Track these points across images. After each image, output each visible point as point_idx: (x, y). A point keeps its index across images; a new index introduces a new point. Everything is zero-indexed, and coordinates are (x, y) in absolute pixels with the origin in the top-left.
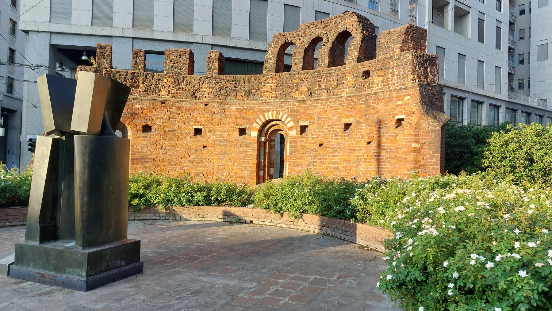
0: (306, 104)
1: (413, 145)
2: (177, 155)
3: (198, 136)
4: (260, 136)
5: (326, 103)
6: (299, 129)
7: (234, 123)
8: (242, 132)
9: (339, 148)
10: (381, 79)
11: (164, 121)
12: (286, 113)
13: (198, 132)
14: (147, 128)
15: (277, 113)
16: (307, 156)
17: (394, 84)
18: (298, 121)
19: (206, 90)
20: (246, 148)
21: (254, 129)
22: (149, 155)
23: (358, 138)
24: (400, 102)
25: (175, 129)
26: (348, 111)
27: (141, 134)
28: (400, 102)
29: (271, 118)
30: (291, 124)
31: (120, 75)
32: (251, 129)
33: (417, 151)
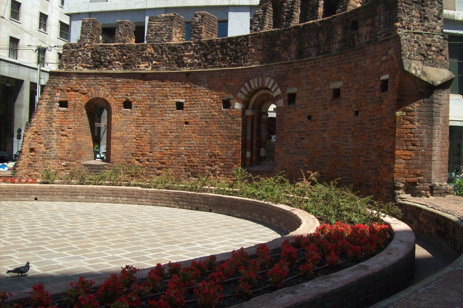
5: (315, 63)
6: (286, 98)
8: (227, 104)
9: (328, 120)
12: (272, 78)
13: (180, 106)
16: (294, 132)
24: (384, 58)
25: (156, 103)
26: (337, 72)
28: (384, 58)
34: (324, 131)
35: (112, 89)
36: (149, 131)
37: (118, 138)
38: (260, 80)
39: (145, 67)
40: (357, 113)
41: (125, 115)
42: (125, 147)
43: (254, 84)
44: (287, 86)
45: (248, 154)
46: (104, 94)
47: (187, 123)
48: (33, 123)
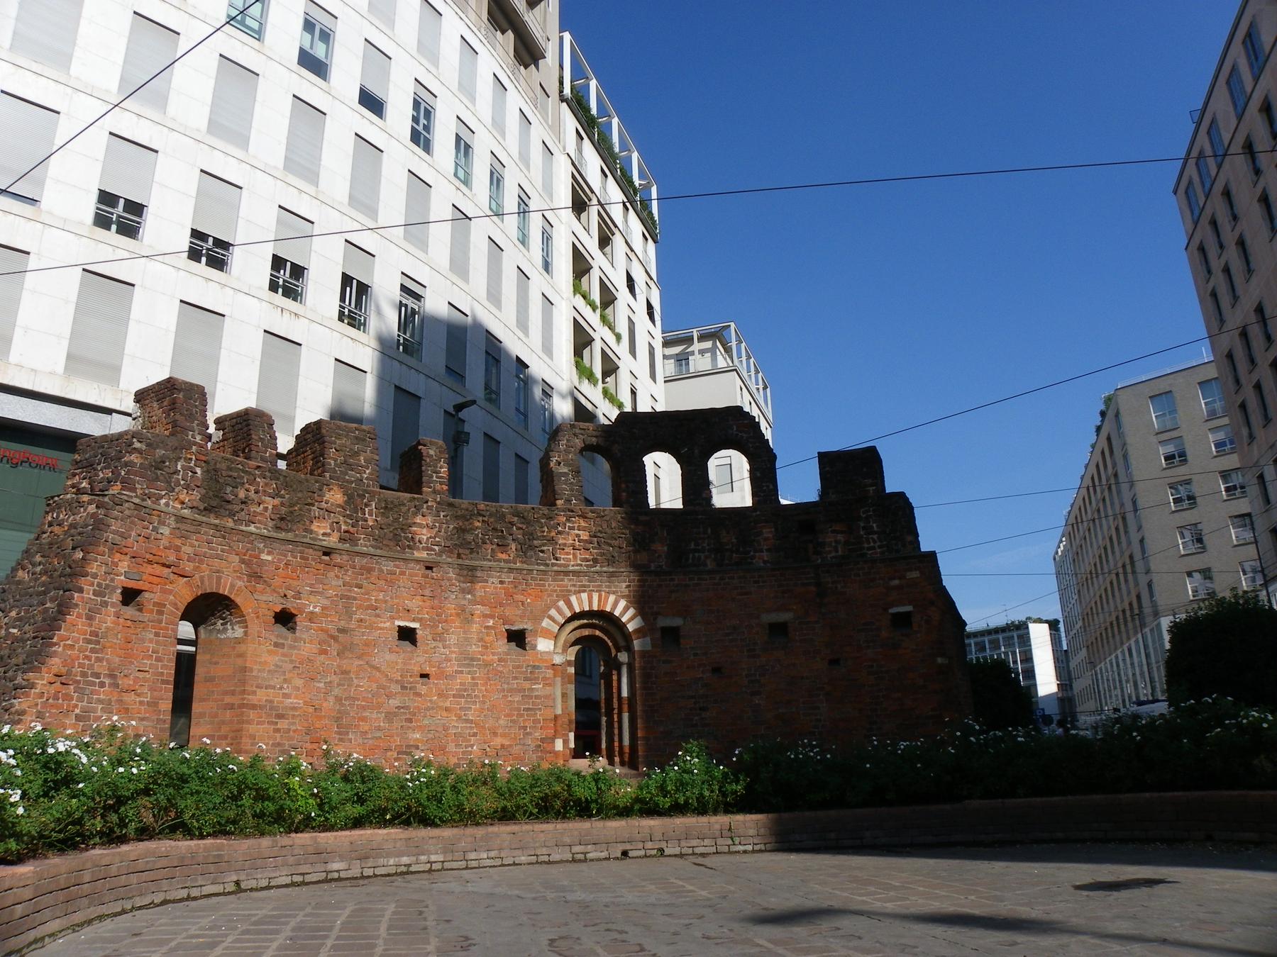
0: (672, 580)
1: (940, 660)
2: (355, 699)
5: (722, 579)
6: (658, 635)
7: (492, 617)
8: (518, 638)
10: (840, 537)
11: (327, 602)
12: (623, 597)
13: (407, 635)
15: (600, 597)
17: (873, 548)
19: (424, 531)
20: (526, 679)
21: (546, 634)
22: (286, 696)
24: (896, 582)
25: (353, 624)
28: (896, 582)
29: (587, 609)
31: (230, 469)
32: (535, 633)
36: (336, 691)
37: (261, 707)
38: (595, 596)
39: (324, 534)
40: (834, 662)
42: (278, 730)
44: (657, 614)
46: (232, 586)
47: (423, 676)
48: (55, 644)
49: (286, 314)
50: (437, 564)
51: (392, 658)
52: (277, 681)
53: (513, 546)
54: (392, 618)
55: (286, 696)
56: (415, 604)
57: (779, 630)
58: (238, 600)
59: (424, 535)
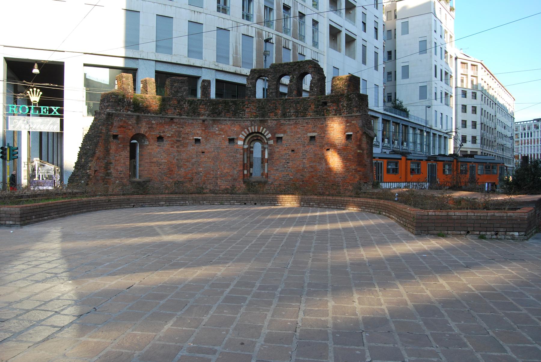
1: (358, 151)
3: (198, 144)
4: (244, 144)
6: (275, 140)
8: (231, 140)
11: (172, 133)
13: (197, 141)
14: (160, 139)
18: (275, 133)
21: (241, 139)
22: (162, 159)
23: (320, 146)
27: (157, 144)
30: (270, 136)
33: (359, 155)
34: (304, 159)
35: (149, 128)
38: (256, 128)
41: (160, 146)
43: (252, 130)
45: (246, 172)
47: (203, 152)
49: (196, 13)
50: (206, 120)
51: (192, 148)
52: (159, 155)
53: (231, 112)
54: (193, 136)
55: (162, 159)
56: (199, 132)
57: (312, 138)
58: (147, 135)
59: (202, 111)
